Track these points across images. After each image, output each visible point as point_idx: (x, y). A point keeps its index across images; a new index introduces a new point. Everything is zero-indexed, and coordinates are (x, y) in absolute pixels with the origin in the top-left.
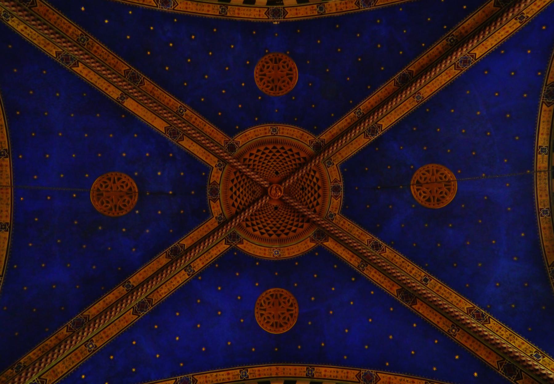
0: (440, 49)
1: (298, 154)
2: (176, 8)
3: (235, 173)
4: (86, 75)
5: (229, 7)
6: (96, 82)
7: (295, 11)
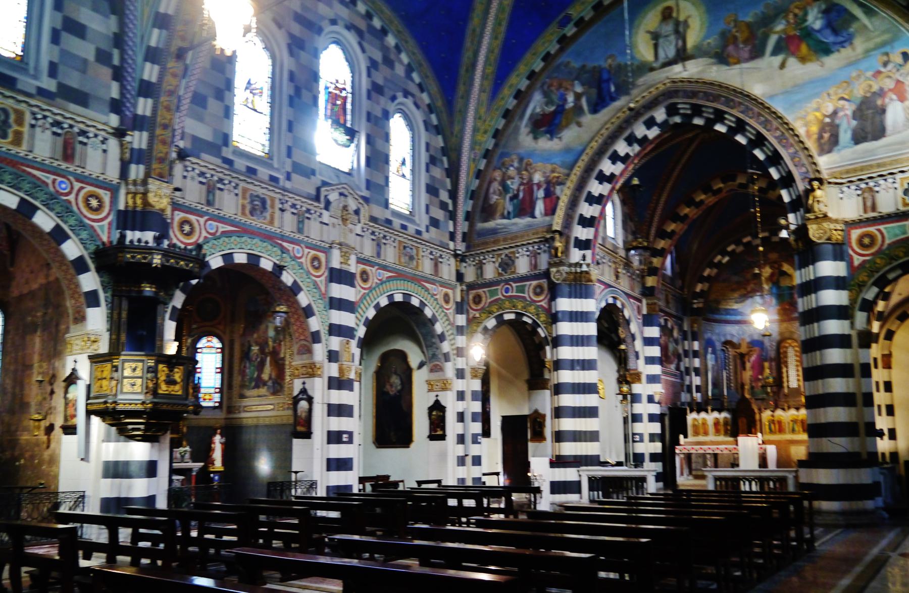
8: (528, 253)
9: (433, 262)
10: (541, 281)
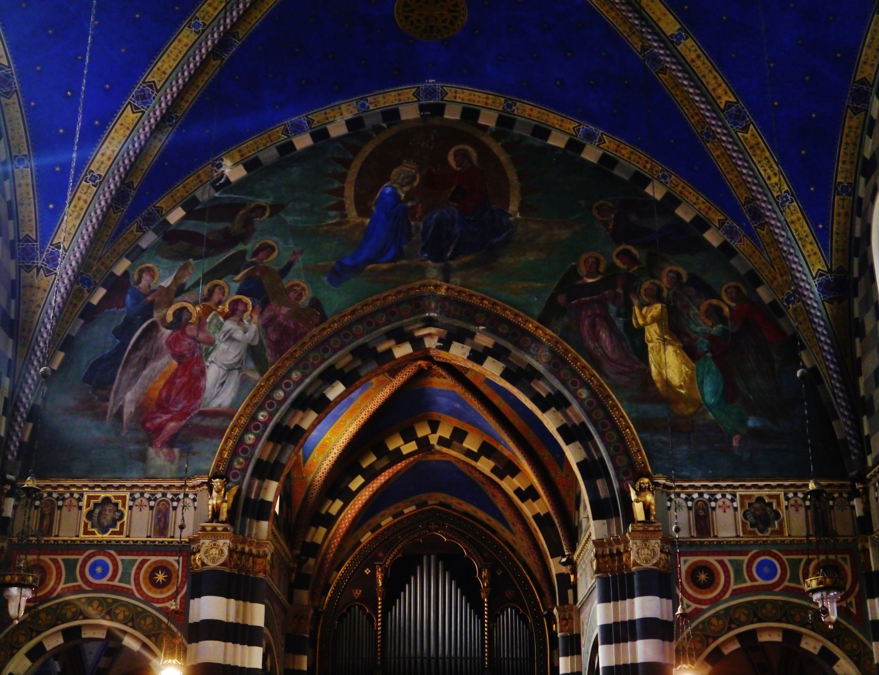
0: (183, 103)
2: (577, 124)
4: (720, 85)
5: (501, 109)
6: (710, 71)
7: (401, 97)
8: (152, 503)
10: (172, 559)
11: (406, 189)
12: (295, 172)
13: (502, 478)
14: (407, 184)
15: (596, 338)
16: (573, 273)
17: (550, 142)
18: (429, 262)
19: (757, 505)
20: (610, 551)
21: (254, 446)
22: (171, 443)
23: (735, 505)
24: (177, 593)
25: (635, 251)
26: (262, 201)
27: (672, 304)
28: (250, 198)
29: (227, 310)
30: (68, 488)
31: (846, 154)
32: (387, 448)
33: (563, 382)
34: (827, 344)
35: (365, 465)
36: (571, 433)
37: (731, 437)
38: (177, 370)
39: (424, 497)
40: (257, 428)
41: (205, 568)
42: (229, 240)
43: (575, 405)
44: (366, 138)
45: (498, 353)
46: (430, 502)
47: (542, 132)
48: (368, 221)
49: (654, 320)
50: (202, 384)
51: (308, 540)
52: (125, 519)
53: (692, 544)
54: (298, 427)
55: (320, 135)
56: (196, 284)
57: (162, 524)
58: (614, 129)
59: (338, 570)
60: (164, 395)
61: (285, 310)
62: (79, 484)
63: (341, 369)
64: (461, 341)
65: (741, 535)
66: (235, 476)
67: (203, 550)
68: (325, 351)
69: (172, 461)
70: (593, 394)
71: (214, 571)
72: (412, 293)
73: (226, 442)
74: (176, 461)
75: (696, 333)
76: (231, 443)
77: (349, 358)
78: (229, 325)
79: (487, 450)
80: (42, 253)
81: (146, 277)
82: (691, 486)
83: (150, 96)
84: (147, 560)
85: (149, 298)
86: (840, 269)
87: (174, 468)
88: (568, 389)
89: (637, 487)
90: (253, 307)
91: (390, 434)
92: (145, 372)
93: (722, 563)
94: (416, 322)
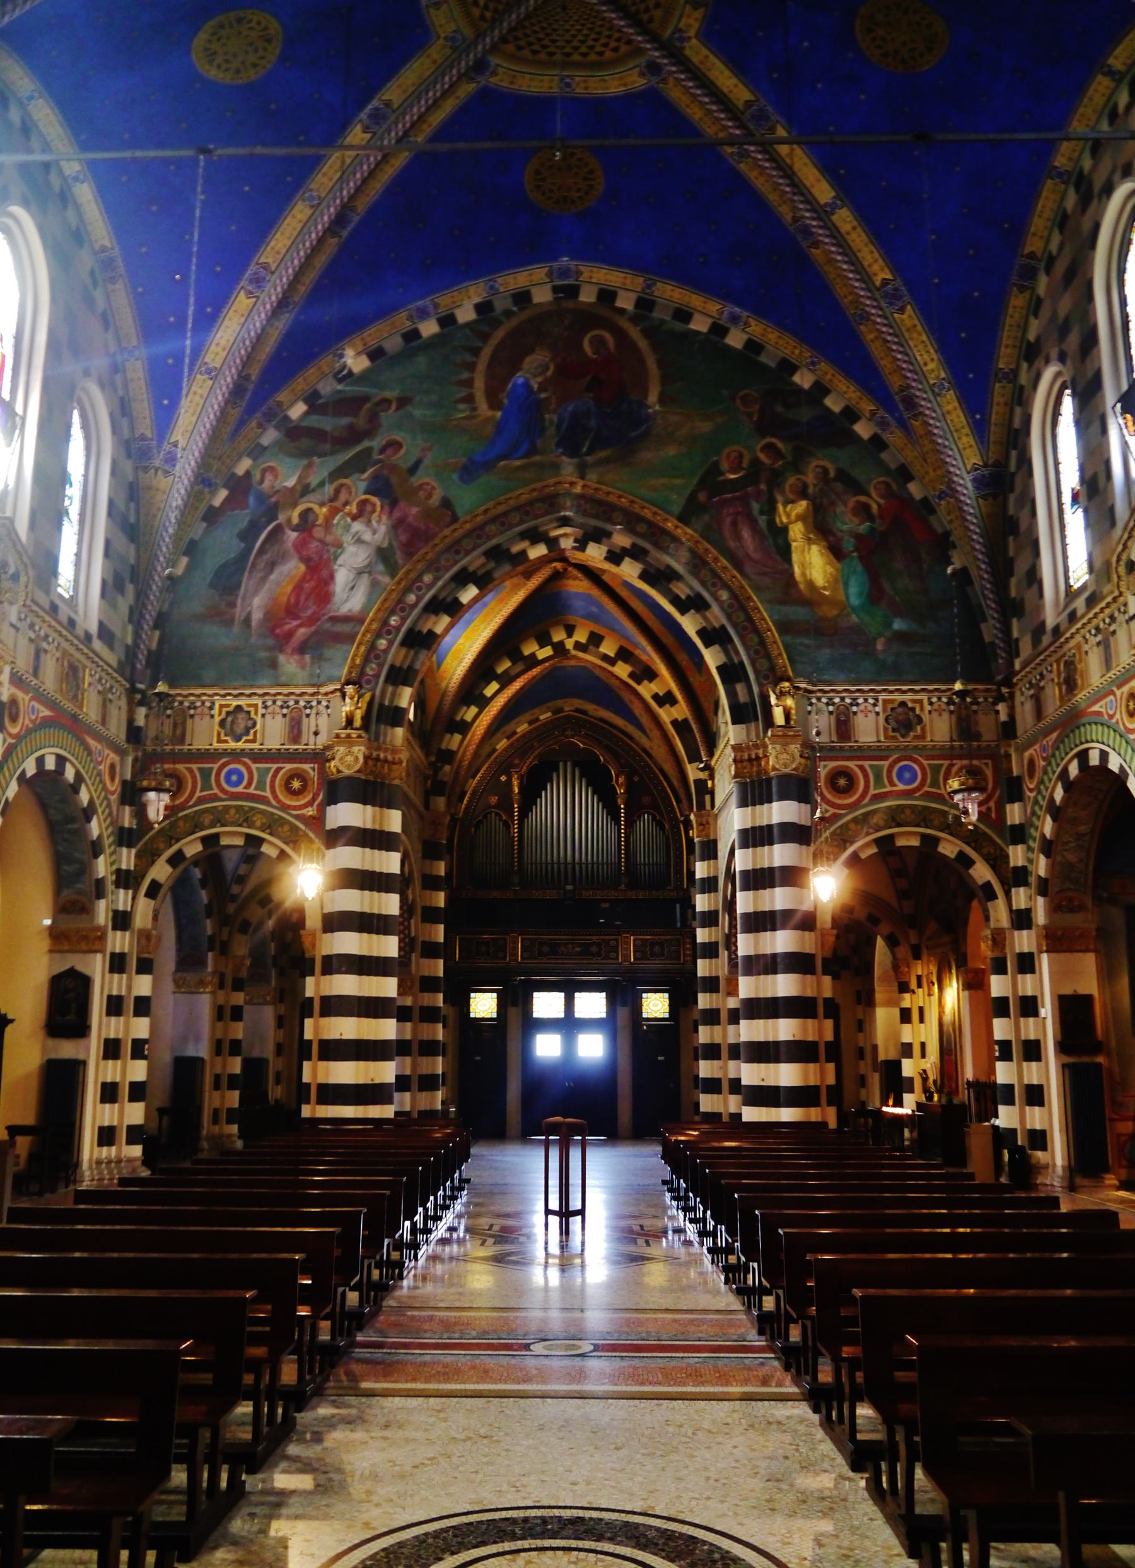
1: (519, 48)
3: (651, 20)
4: (876, 261)
8: (285, 711)
9: (100, 698)
10: (307, 767)
11: (539, 379)
12: (422, 361)
13: (639, 683)
14: (540, 374)
15: (738, 538)
16: (714, 470)
17: (693, 326)
18: (564, 458)
19: (900, 710)
20: (749, 755)
21: (386, 651)
22: (301, 650)
23: (877, 709)
24: (314, 799)
25: (780, 445)
26: (387, 394)
27: (818, 501)
28: (375, 391)
29: (355, 511)
30: (199, 696)
31: (1009, 337)
32: (521, 653)
33: (704, 584)
34: (979, 543)
35: (500, 670)
36: (710, 636)
37: (875, 639)
38: (305, 574)
39: (559, 703)
40: (389, 633)
41: (341, 775)
42: (353, 436)
43: (715, 608)
44: (496, 324)
45: (636, 553)
46: (566, 709)
47: (683, 315)
48: (499, 414)
49: (799, 518)
50: (331, 587)
51: (443, 746)
52: (258, 727)
53: (832, 748)
54: (431, 633)
55: (447, 321)
56: (322, 484)
57: (296, 731)
58: (762, 311)
59: (474, 777)
60: (292, 600)
61: (414, 510)
62: (210, 692)
63: (474, 572)
64: (598, 541)
65: (882, 739)
66: (369, 682)
67: (338, 757)
68: (457, 552)
69: (303, 667)
70: (734, 595)
71: (349, 779)
72: (547, 491)
73: (358, 648)
74: (308, 668)
75: (841, 531)
76: (363, 649)
77: (483, 560)
78: (357, 526)
79: (624, 655)
80: (159, 452)
81: (269, 477)
82: (833, 691)
83: (264, 279)
84: (282, 768)
85: (273, 499)
86: (997, 464)
87: (305, 674)
88: (708, 590)
89: (778, 691)
90: (382, 507)
91: (524, 639)
92: (273, 577)
93: (861, 768)
94: (551, 521)
